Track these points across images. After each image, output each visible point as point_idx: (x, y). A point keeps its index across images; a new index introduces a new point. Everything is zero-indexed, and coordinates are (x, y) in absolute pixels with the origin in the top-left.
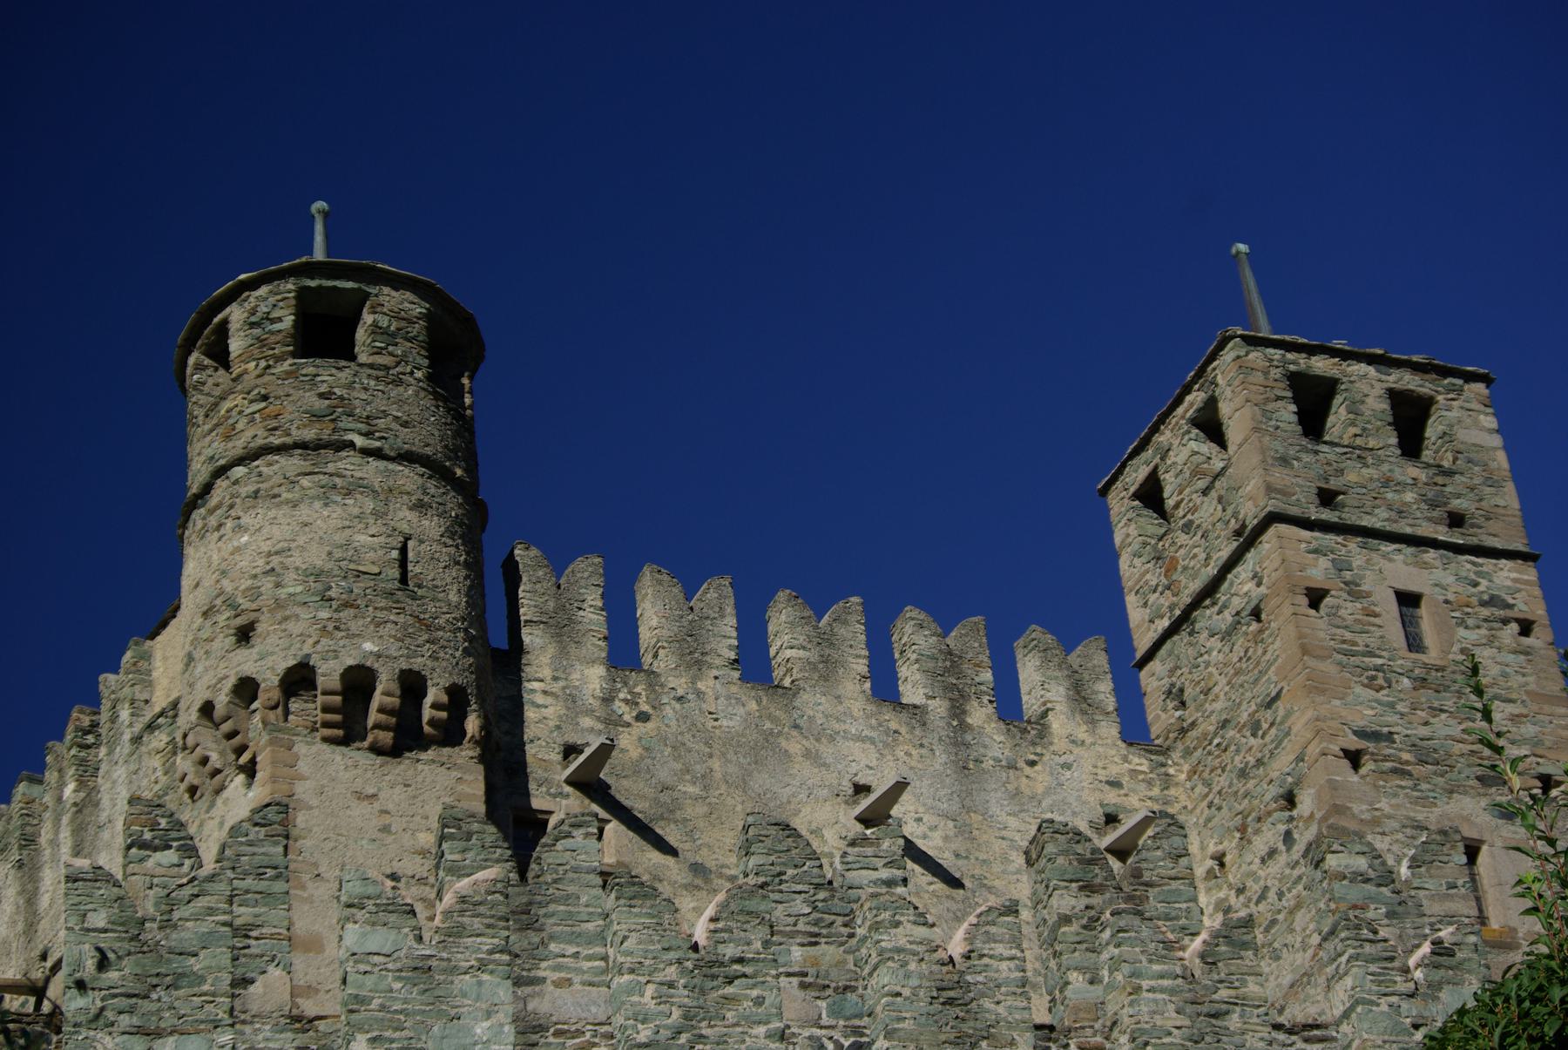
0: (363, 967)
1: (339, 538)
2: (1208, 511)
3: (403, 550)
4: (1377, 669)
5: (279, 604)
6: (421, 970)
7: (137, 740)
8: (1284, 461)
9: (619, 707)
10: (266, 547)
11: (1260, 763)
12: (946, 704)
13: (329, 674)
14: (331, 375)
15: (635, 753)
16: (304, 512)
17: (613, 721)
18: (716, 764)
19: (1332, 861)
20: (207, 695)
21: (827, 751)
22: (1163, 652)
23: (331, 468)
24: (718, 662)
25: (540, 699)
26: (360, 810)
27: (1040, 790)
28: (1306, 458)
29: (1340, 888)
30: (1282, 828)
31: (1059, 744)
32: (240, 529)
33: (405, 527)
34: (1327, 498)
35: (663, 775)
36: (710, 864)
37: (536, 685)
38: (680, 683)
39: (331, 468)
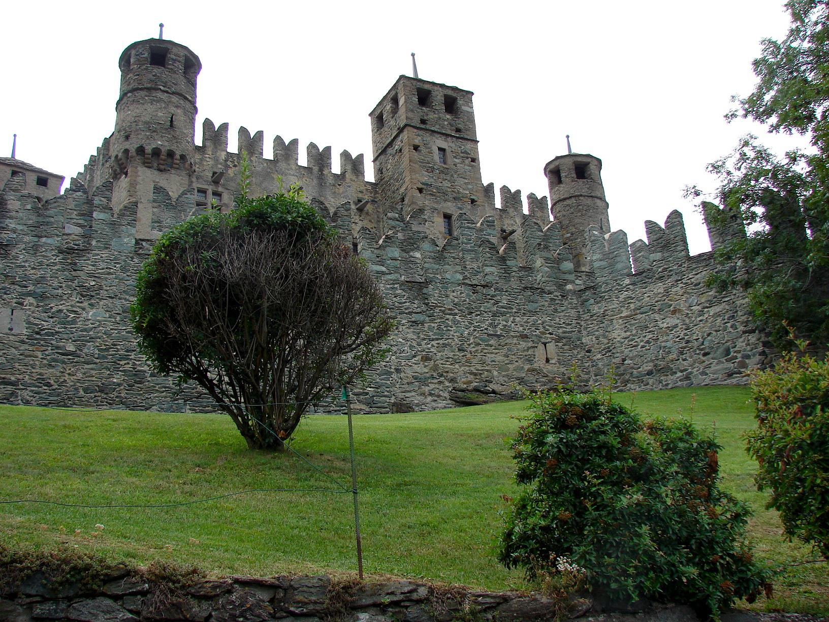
0: (97, 223)
2: (392, 123)
3: (172, 118)
6: (113, 224)
7: (103, 165)
8: (412, 111)
9: (229, 163)
10: (135, 115)
11: (397, 189)
12: (318, 168)
14: (157, 70)
15: (232, 175)
16: (146, 106)
17: (227, 167)
18: (254, 179)
19: (389, 214)
20: (117, 153)
22: (379, 158)
23: (154, 95)
24: (257, 153)
25: (208, 160)
27: (341, 191)
29: (390, 222)
30: (401, 206)
31: (348, 180)
32: (129, 110)
33: (173, 112)
34: (423, 122)
37: (207, 156)
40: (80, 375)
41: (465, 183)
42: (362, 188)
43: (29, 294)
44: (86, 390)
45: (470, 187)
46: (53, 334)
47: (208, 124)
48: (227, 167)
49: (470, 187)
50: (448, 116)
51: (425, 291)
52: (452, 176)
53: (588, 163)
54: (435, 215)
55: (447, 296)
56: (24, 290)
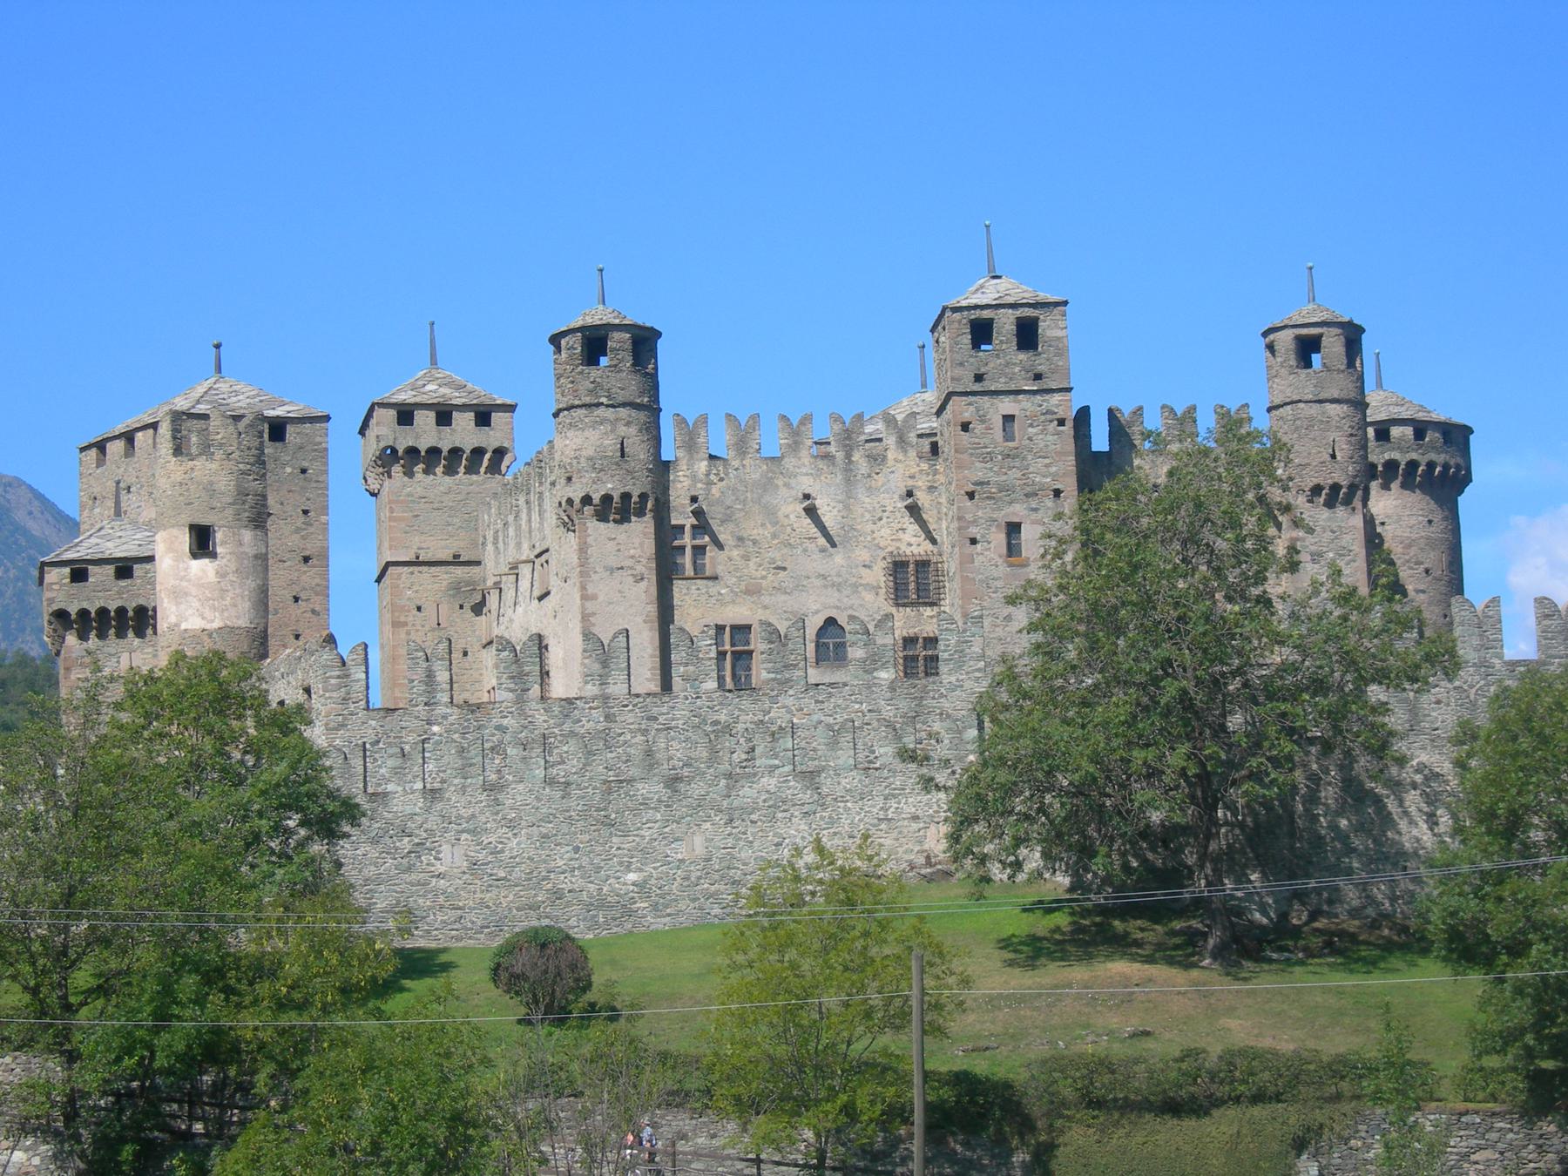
1: (598, 443)
3: (622, 444)
4: (987, 453)
5: (579, 471)
9: (712, 477)
13: (596, 498)
16: (586, 433)
17: (710, 483)
18: (749, 495)
21: (793, 482)
25: (682, 479)
26: (611, 545)
27: (880, 484)
28: (972, 360)
31: (890, 462)
35: (728, 503)
36: (745, 535)
38: (736, 463)
39: (595, 414)
40: (511, 897)
41: (1047, 466)
42: (913, 471)
43: (463, 831)
44: (518, 909)
45: (1053, 469)
46: (486, 864)
47: (680, 421)
48: (710, 484)
49: (1053, 469)
50: (1022, 356)
51: (817, 780)
52: (1024, 458)
53: (1321, 336)
54: (993, 529)
55: (839, 783)
56: (460, 828)
